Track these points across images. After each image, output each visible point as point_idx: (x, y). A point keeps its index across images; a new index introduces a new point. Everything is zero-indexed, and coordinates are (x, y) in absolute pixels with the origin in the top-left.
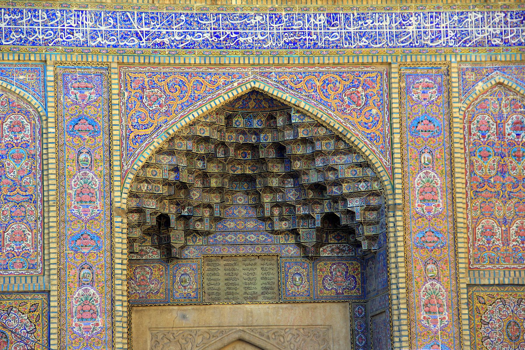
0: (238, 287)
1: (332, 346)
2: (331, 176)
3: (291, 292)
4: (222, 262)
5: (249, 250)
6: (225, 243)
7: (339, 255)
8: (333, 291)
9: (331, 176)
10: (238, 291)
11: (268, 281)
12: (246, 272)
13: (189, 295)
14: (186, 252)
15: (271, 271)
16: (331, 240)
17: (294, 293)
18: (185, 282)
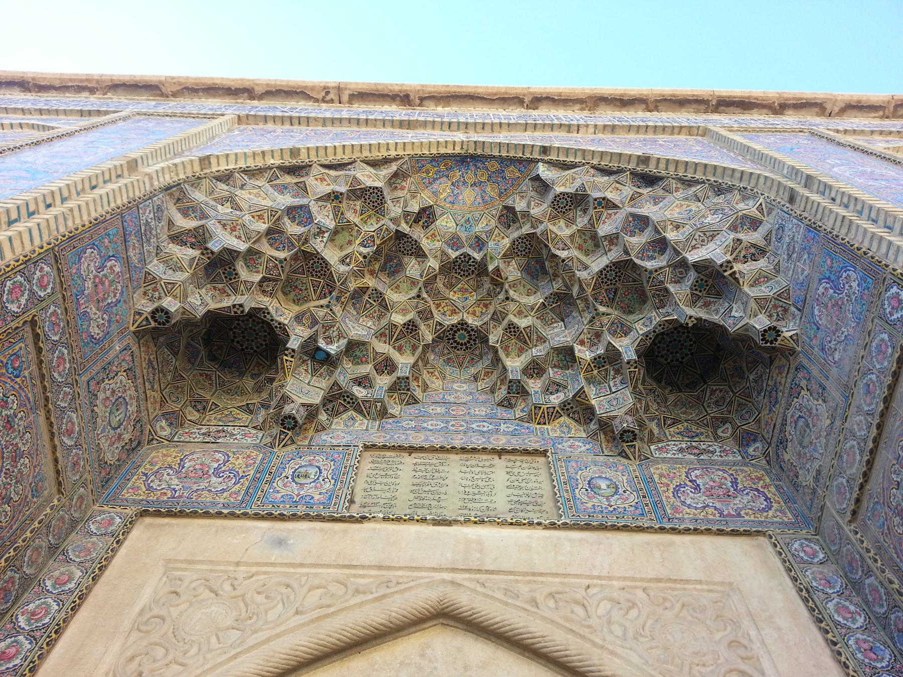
0: (443, 497)
1: (753, 633)
2: (637, 241)
3: (589, 505)
4: (409, 460)
5: (478, 442)
6: (417, 429)
7: (702, 457)
8: (710, 510)
9: (637, 241)
10: (443, 504)
11: (525, 491)
12: (469, 476)
13: (308, 499)
14: (324, 437)
15: (534, 479)
16: (672, 436)
17: (598, 509)
18: (306, 476)
